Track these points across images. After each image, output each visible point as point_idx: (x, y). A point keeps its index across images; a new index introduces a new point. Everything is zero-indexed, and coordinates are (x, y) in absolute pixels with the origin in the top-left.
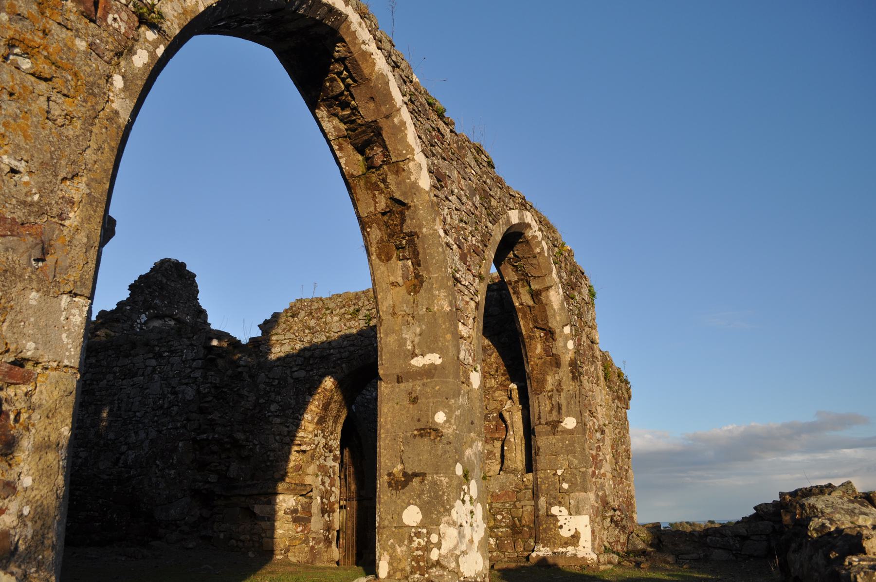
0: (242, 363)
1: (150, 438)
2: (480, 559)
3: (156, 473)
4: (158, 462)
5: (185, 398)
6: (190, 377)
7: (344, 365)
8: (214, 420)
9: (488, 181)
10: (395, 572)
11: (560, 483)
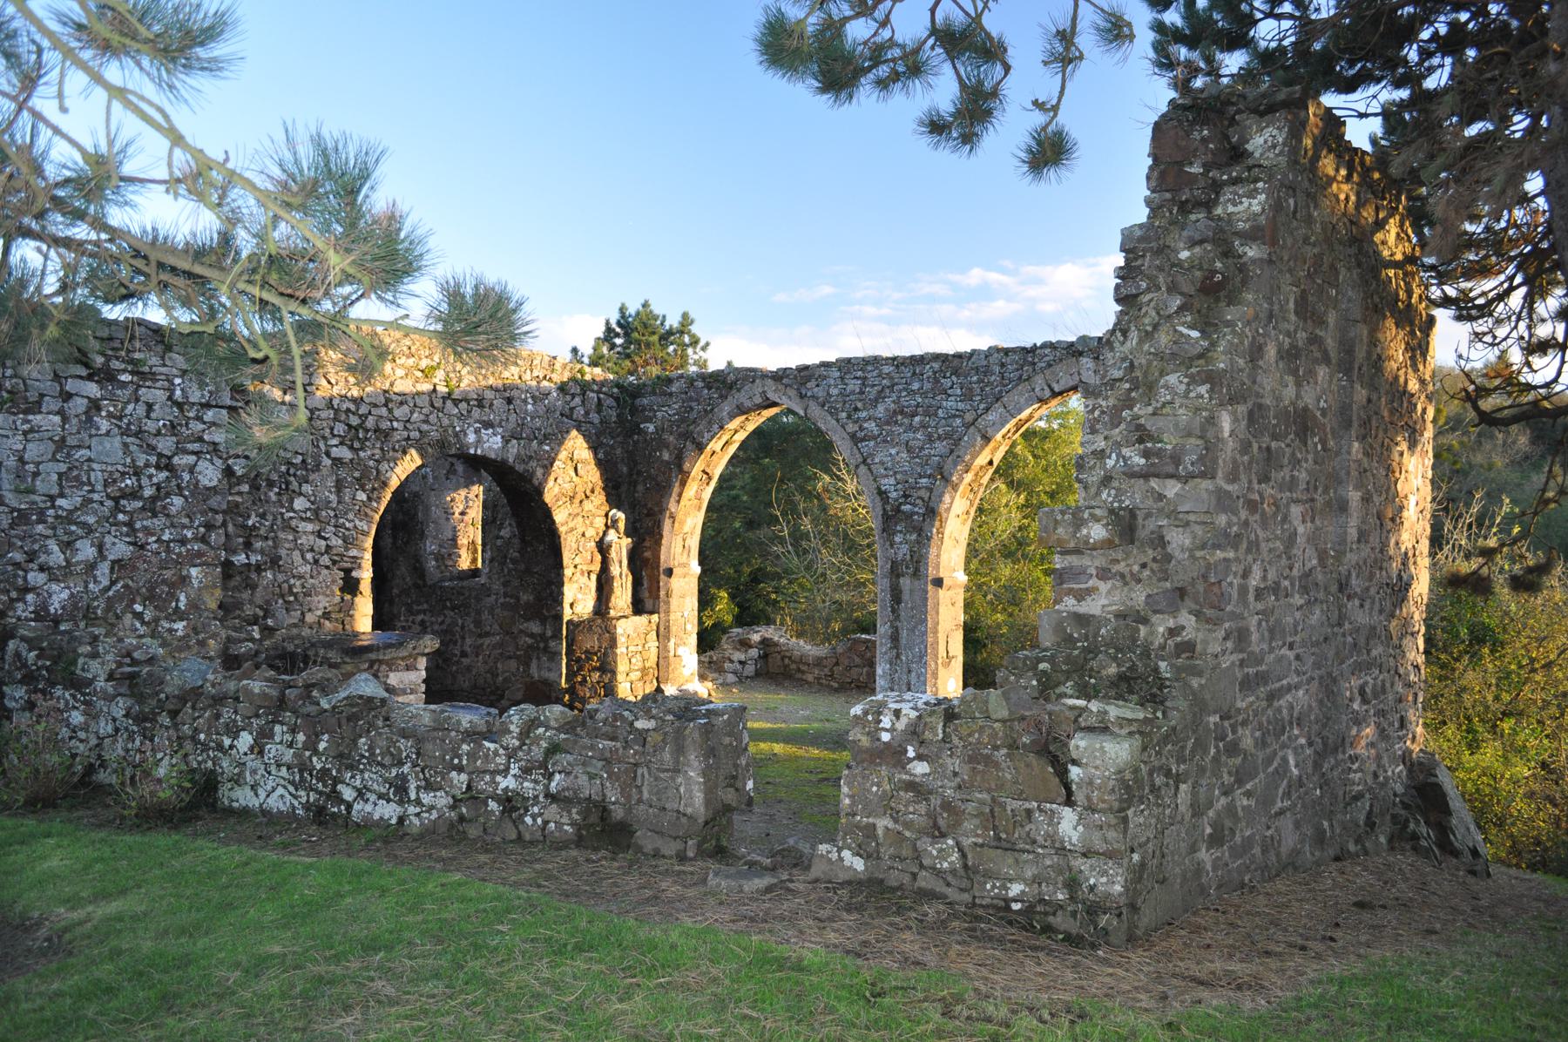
1: (111, 557)
3: (137, 630)
5: (198, 481)
6: (200, 439)
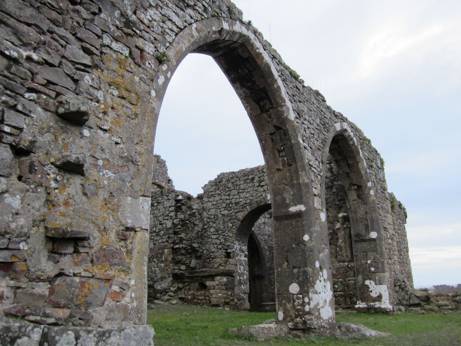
0: (195, 207)
2: (330, 310)
4: (155, 260)
7: (248, 207)
8: (182, 238)
9: (323, 110)
10: (287, 317)
11: (370, 268)
